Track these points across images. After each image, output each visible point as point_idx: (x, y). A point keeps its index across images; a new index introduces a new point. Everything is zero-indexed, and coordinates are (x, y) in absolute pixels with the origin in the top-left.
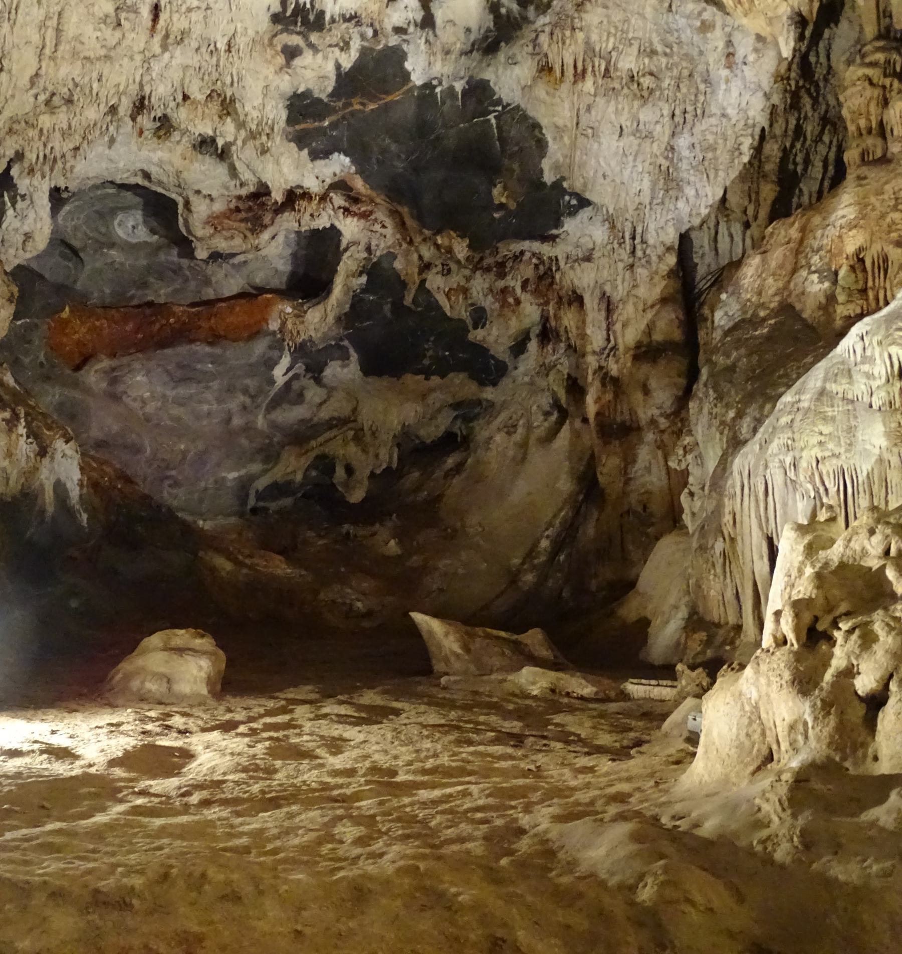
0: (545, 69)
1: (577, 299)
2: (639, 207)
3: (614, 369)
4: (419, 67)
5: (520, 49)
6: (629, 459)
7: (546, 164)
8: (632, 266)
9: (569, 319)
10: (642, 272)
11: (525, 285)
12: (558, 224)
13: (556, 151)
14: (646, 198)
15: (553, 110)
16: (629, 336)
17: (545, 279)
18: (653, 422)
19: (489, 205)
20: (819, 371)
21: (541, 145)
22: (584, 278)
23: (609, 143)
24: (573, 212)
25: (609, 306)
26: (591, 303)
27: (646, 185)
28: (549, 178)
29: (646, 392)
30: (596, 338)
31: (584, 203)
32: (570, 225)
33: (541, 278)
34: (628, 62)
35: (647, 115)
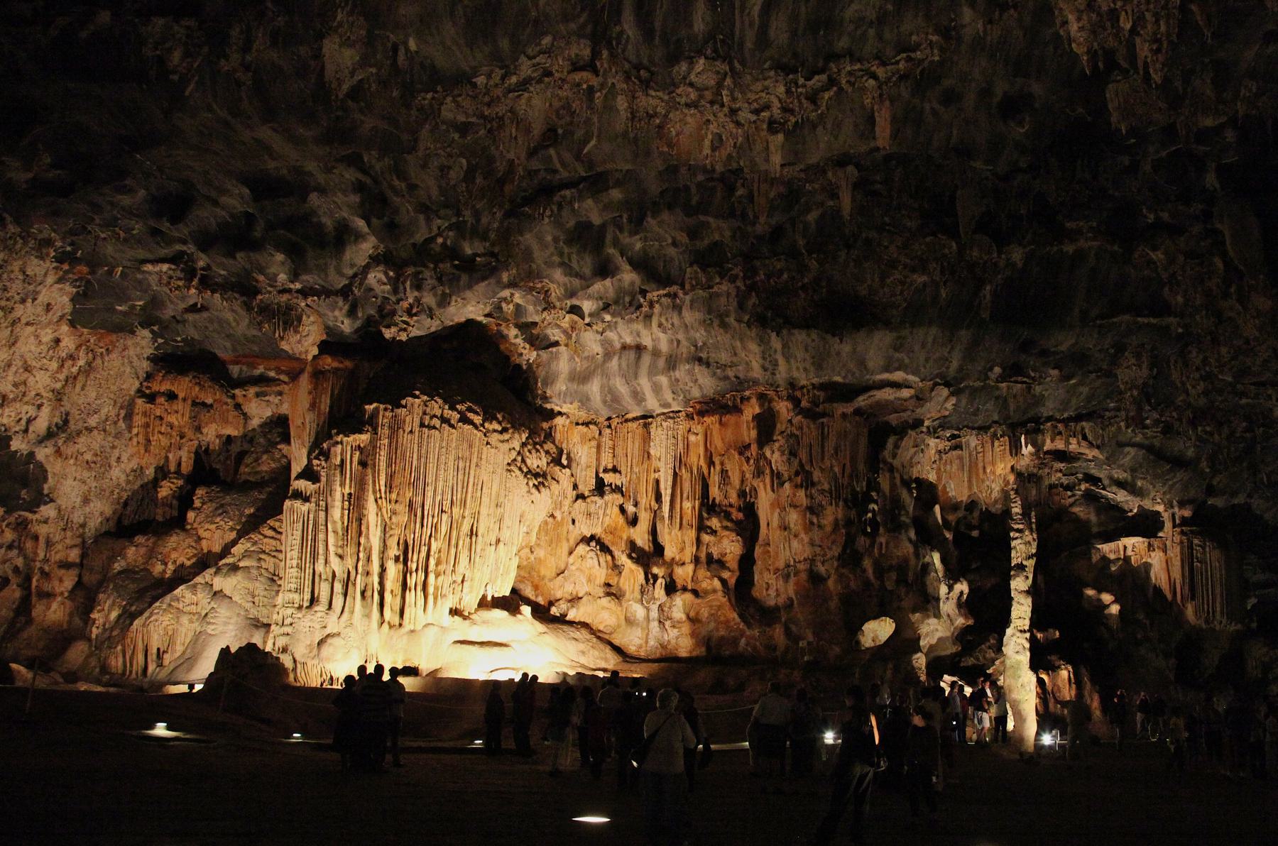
0: (58, 452)
1: (36, 538)
2: (74, 508)
3: (47, 568)
4: (17, 444)
5: (50, 443)
6: (49, 608)
7: (46, 486)
8: (64, 530)
9: (29, 545)
10: (69, 534)
11: (7, 526)
12: (38, 506)
13: (51, 481)
14: (77, 505)
15: (54, 467)
16: (56, 557)
17: (22, 526)
18: (62, 593)
19: (19, 498)
20: (168, 598)
21: (46, 479)
22: (43, 530)
23: (70, 482)
24: (46, 503)
25: (49, 544)
26: (42, 540)
27: (79, 500)
28: (46, 492)
29: (61, 580)
30: (41, 555)
31: (52, 501)
32: (42, 508)
33: (18, 524)
34: (88, 457)
35: (86, 474)
